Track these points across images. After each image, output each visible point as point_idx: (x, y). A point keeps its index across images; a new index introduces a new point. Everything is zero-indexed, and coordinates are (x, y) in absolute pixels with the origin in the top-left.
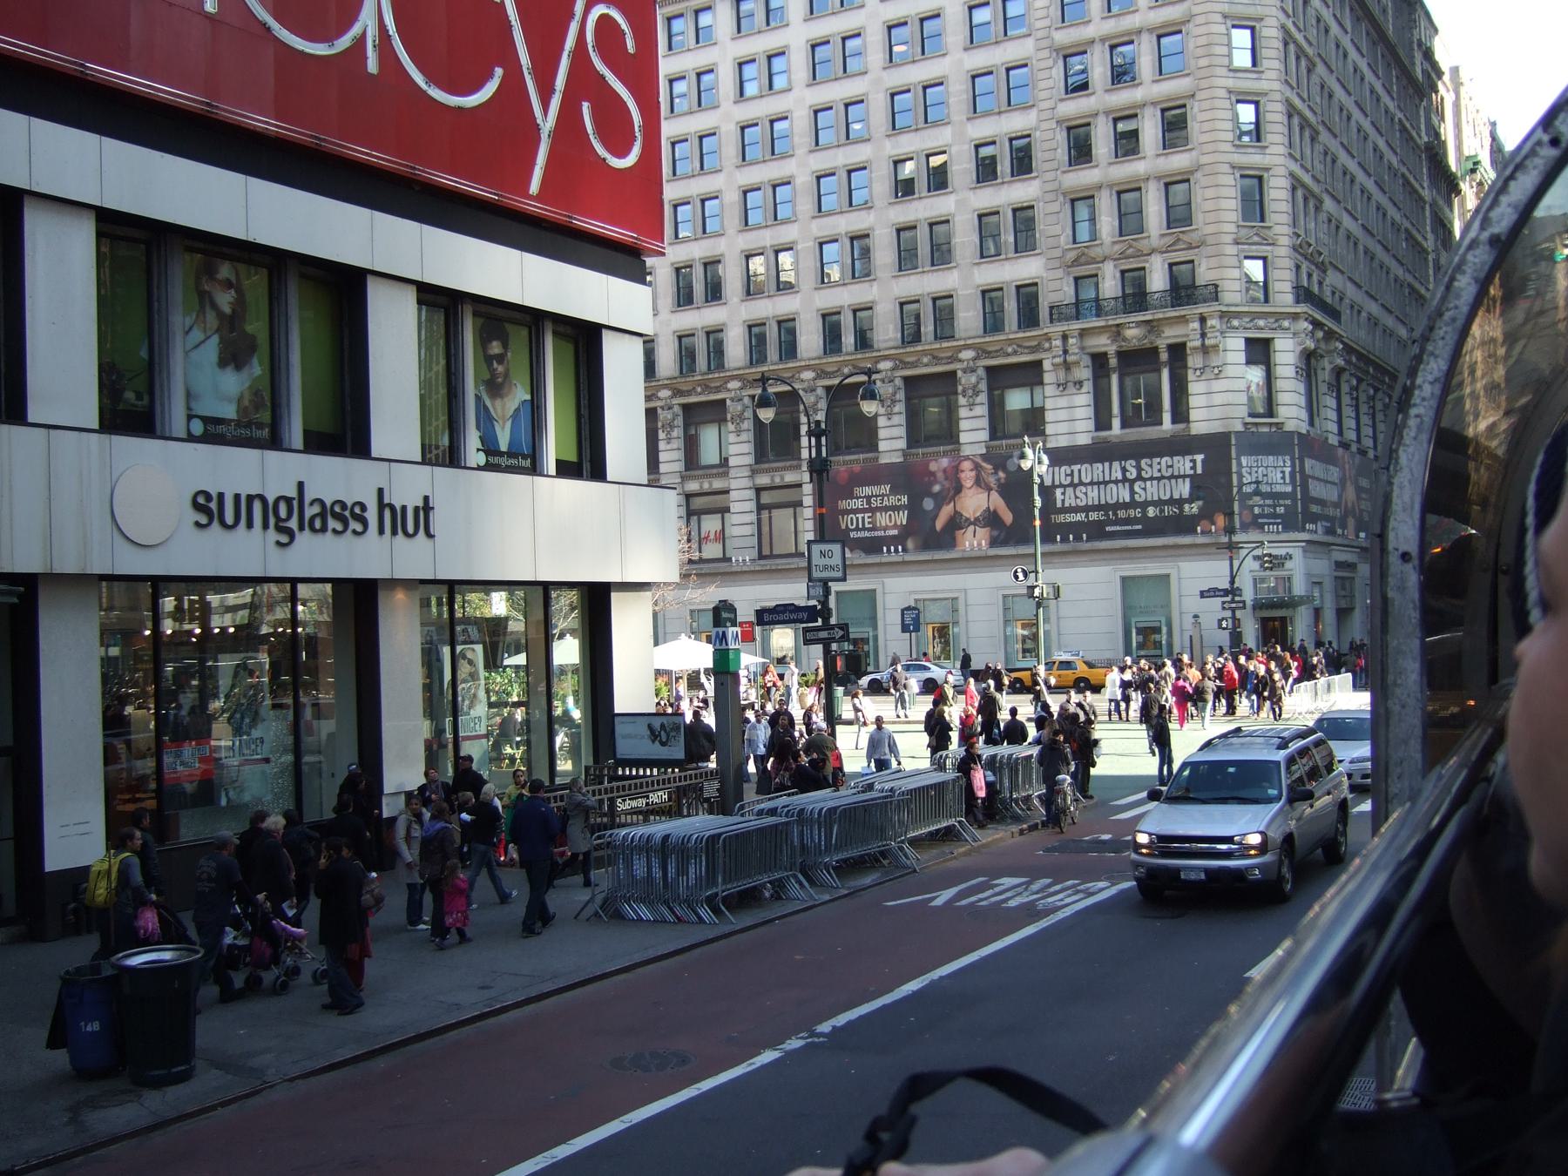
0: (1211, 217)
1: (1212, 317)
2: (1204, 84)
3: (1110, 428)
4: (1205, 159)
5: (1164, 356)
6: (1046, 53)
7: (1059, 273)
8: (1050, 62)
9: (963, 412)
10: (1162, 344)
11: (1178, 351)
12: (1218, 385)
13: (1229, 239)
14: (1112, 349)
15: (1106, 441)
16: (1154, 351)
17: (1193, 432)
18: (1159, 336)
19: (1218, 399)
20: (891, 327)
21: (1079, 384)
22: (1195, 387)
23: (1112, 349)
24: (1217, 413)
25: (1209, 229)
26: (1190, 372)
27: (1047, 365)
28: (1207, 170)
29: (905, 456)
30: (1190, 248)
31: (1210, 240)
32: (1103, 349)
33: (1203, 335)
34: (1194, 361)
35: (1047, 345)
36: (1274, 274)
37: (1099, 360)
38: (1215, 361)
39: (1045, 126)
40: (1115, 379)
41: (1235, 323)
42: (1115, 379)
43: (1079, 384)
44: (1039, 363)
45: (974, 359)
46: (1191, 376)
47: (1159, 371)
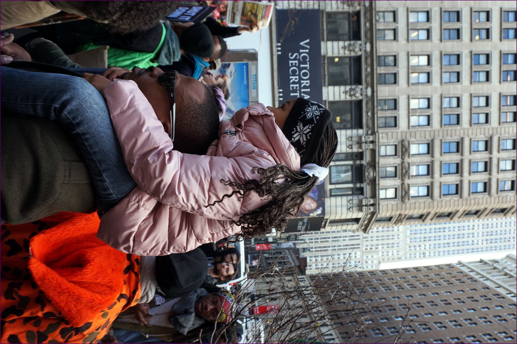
0: (413, 206)
2: (464, 202)
4: (435, 203)
5: (358, 185)
6: (491, 133)
7: (400, 138)
8: (487, 134)
9: (343, 88)
10: (364, 185)
11: (361, 191)
13: (402, 212)
14: (364, 162)
16: (361, 182)
18: (368, 184)
20: (385, 50)
21: (352, 148)
22: (345, 199)
23: (364, 162)
24: (333, 209)
25: (408, 205)
27: (361, 132)
28: (431, 204)
29: (324, 56)
30: (402, 197)
31: (404, 205)
32: (364, 158)
33: (366, 205)
34: (355, 200)
35: (370, 132)
37: (360, 156)
39: (462, 131)
40: (351, 162)
41: (369, 216)
42: (351, 162)
43: (351, 147)
44: (361, 127)
45: (366, 95)
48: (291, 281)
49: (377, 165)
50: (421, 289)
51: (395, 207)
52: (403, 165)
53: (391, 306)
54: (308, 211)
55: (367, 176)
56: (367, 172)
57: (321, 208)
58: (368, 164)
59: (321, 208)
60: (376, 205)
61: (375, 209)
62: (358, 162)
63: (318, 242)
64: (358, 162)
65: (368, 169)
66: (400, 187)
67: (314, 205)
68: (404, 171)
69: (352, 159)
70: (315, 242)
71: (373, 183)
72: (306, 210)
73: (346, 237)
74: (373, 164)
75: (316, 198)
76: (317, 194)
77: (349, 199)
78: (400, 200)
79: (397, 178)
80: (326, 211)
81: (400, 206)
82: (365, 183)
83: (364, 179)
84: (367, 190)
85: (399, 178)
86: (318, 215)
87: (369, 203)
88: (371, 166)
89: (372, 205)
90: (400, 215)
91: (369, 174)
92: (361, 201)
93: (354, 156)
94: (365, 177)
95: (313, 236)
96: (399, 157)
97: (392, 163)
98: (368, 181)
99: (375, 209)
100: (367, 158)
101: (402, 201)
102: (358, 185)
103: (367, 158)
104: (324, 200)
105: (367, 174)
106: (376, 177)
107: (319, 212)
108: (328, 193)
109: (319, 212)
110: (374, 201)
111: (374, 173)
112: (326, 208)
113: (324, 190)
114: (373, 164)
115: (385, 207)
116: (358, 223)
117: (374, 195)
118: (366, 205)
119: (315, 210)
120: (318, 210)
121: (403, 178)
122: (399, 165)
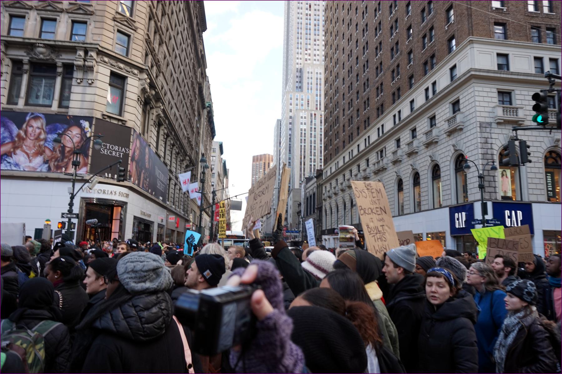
1: (92, 51)
3: (16, 104)
10: (59, 62)
11: (69, 68)
12: (89, 90)
13: (111, 17)
14: (26, 59)
15: (11, 111)
17: (70, 114)
19: (88, 98)
22: (75, 89)
23: (26, 59)
24: (86, 105)
26: (74, 80)
30: (86, 14)
31: (98, 13)
32: (21, 58)
34: (78, 75)
36: (132, 45)
37: (17, 63)
38: (90, 76)
40: (25, 78)
41: (106, 59)
42: (25, 78)
46: (74, 82)
47: (54, 78)
48: (326, 187)
49: (27, 41)
50: (339, 40)
51: (98, 25)
52: (40, 8)
53: (349, 71)
54: (82, 139)
55: (44, 56)
56: (38, 56)
57: (81, 121)
58: (28, 54)
59: (81, 121)
60: (85, 47)
61: (92, 49)
62: (26, 67)
63: (315, 159)
64: (26, 67)
65: (35, 54)
66: (70, 15)
67: (75, 131)
68: (49, 8)
69: (21, 75)
70: (314, 162)
71: (56, 48)
72: (80, 142)
73: (321, 129)
74: (30, 47)
75: (66, 126)
76: (59, 125)
77: (76, 84)
78: (90, 16)
79: (58, 18)
80: (87, 115)
81: (98, 18)
82: (57, 60)
83: (50, 61)
84: (66, 58)
85: (59, 16)
86: (90, 127)
87: (83, 57)
88: (32, 50)
89: (86, 53)
90: (114, 19)
91: (42, 53)
92: (79, 67)
93: (18, 72)
94: (47, 60)
95: (318, 164)
96: (28, 13)
97: (35, 22)
98: (53, 56)
99: (92, 49)
100: (20, 54)
101: (91, 15)
102: (60, 70)
103: (20, 54)
104: (70, 116)
105: (41, 56)
106: (44, 44)
107: (86, 124)
108: (63, 110)
109: (86, 124)
110: (80, 50)
111: (39, 47)
112: (79, 115)
113: (56, 114)
114: (29, 46)
115: (96, 37)
116: (127, 77)
117: (73, 50)
118: (85, 60)
119: (82, 129)
120: (83, 125)
121: (58, 10)
122: (38, 14)
